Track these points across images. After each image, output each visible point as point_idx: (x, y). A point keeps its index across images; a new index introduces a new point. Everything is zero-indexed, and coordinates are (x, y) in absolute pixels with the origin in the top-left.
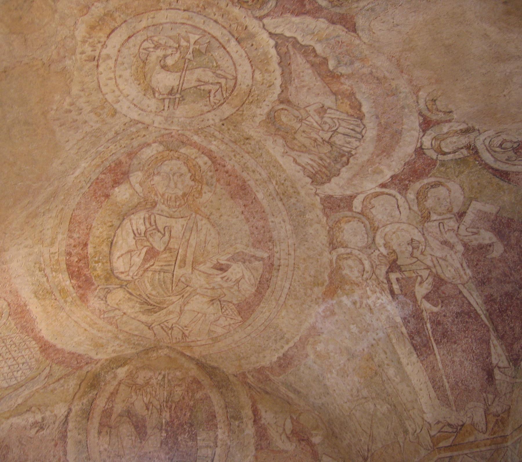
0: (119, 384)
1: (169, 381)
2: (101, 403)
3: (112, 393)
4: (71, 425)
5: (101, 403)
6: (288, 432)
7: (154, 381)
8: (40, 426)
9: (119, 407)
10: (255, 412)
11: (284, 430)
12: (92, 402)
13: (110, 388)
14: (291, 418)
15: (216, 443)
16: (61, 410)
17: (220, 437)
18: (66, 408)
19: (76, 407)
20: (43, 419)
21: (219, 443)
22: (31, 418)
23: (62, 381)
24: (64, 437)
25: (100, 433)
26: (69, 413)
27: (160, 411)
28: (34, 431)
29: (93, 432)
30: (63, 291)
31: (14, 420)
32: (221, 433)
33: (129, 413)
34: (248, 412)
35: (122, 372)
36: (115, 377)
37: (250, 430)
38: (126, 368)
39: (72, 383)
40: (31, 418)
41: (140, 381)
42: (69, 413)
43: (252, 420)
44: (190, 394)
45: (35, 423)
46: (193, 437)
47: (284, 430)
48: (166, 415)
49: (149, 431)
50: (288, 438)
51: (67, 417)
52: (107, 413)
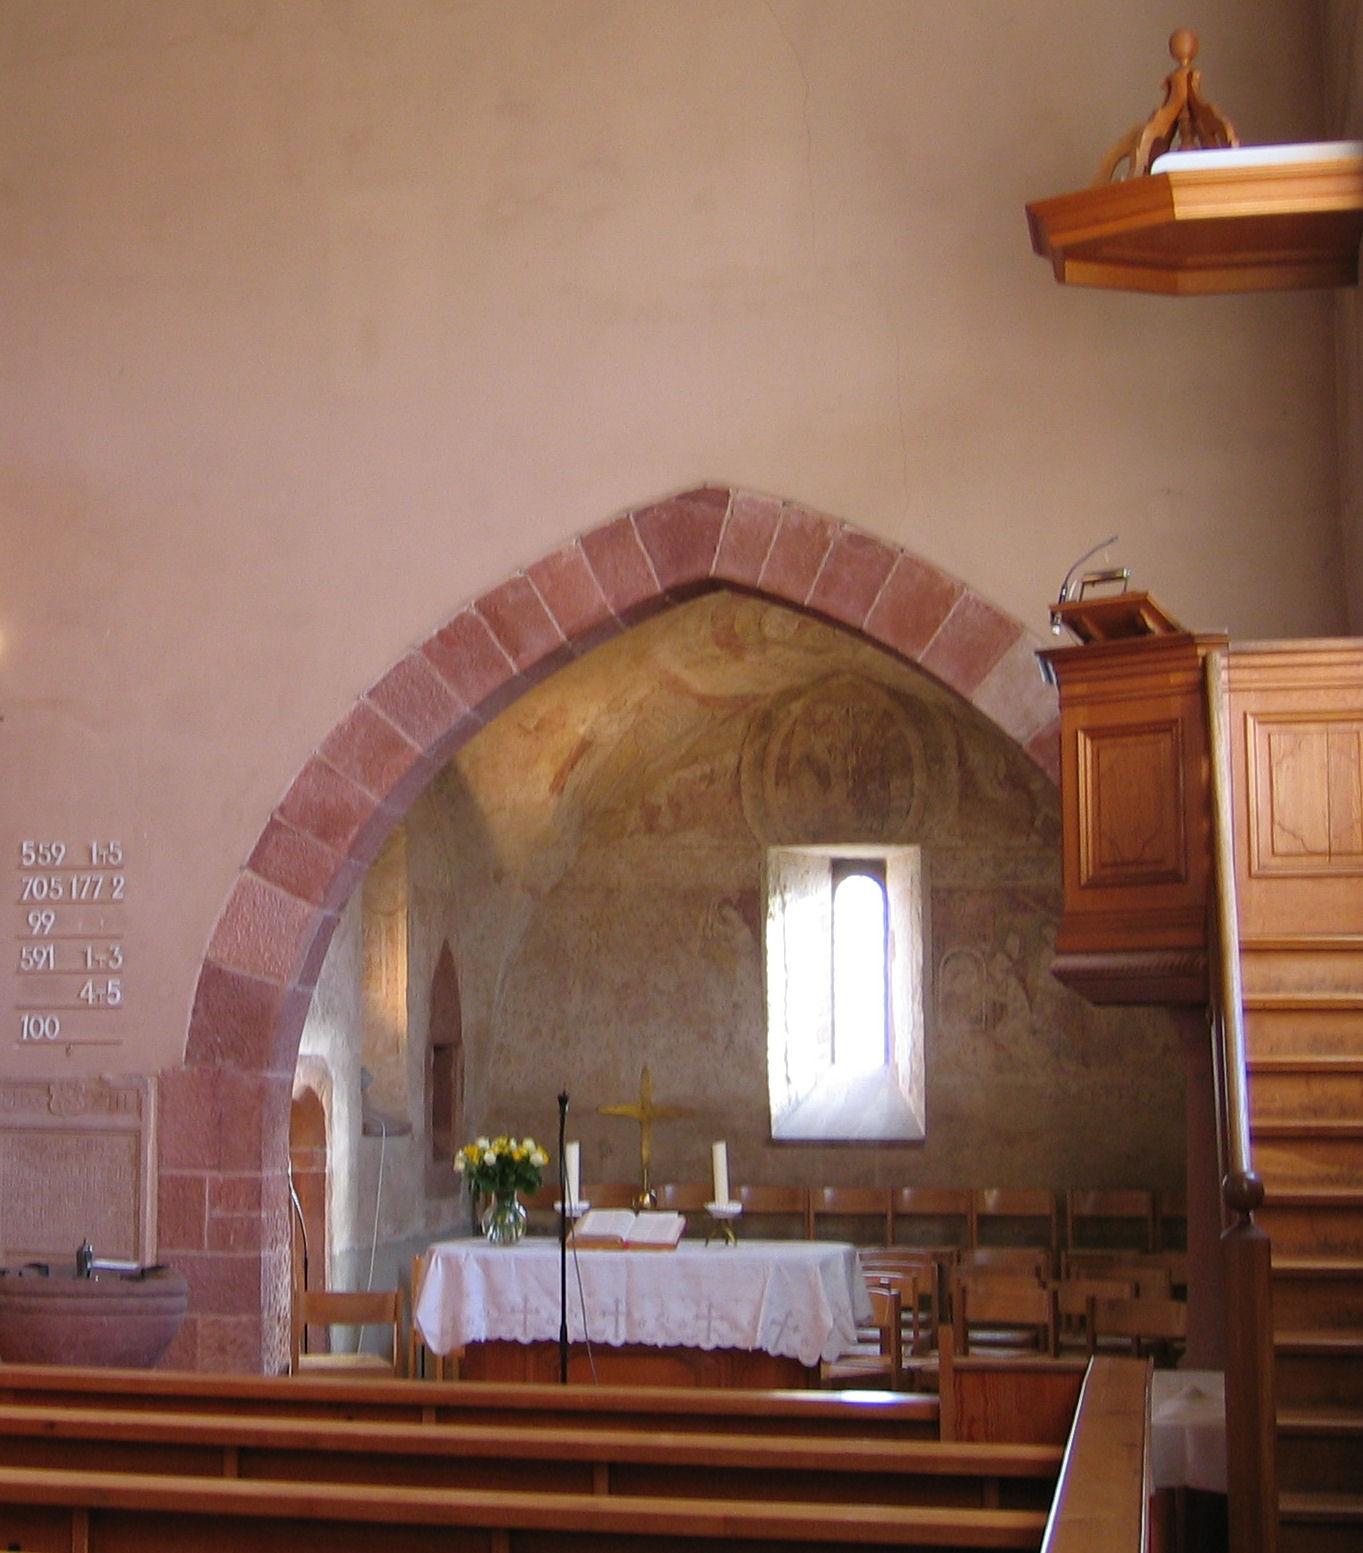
0: (795, 723)
1: (854, 717)
2: (775, 749)
3: (787, 736)
4: (744, 777)
5: (775, 749)
6: (1001, 776)
7: (835, 718)
8: (710, 779)
9: (797, 751)
10: (961, 752)
11: (996, 774)
12: (765, 747)
13: (784, 730)
14: (1006, 759)
15: (912, 795)
16: (730, 759)
17: (917, 784)
18: (737, 756)
19: (748, 756)
20: (712, 770)
21: (916, 792)
22: (698, 770)
23: (727, 723)
24: (738, 792)
25: (777, 784)
26: (740, 763)
27: (845, 757)
28: (703, 787)
29: (770, 782)
30: (717, 658)
31: (685, 774)
32: (919, 780)
33: (808, 760)
34: (951, 752)
35: (797, 707)
36: (789, 712)
37: (954, 774)
38: (801, 701)
39: (739, 727)
40: (698, 770)
41: (819, 717)
42: (740, 763)
43: (957, 763)
44: (880, 733)
45: (703, 777)
46: (885, 786)
47: (996, 774)
48: (852, 760)
49: (834, 781)
50: (1000, 784)
51: (738, 769)
52: (784, 761)
